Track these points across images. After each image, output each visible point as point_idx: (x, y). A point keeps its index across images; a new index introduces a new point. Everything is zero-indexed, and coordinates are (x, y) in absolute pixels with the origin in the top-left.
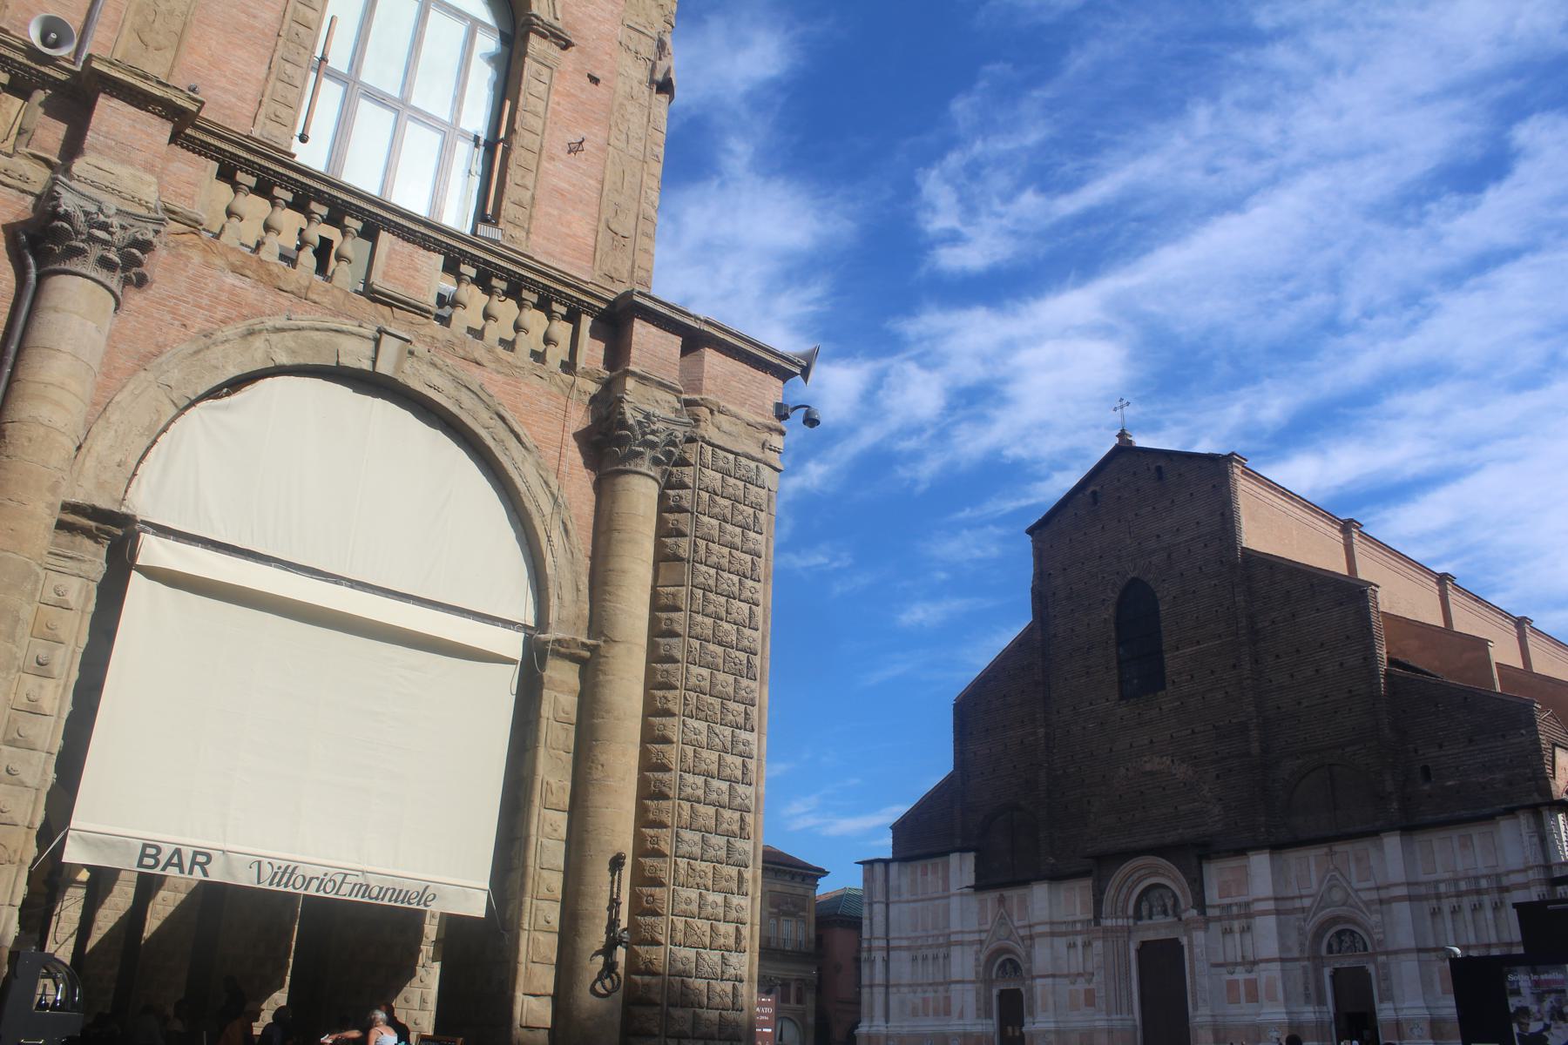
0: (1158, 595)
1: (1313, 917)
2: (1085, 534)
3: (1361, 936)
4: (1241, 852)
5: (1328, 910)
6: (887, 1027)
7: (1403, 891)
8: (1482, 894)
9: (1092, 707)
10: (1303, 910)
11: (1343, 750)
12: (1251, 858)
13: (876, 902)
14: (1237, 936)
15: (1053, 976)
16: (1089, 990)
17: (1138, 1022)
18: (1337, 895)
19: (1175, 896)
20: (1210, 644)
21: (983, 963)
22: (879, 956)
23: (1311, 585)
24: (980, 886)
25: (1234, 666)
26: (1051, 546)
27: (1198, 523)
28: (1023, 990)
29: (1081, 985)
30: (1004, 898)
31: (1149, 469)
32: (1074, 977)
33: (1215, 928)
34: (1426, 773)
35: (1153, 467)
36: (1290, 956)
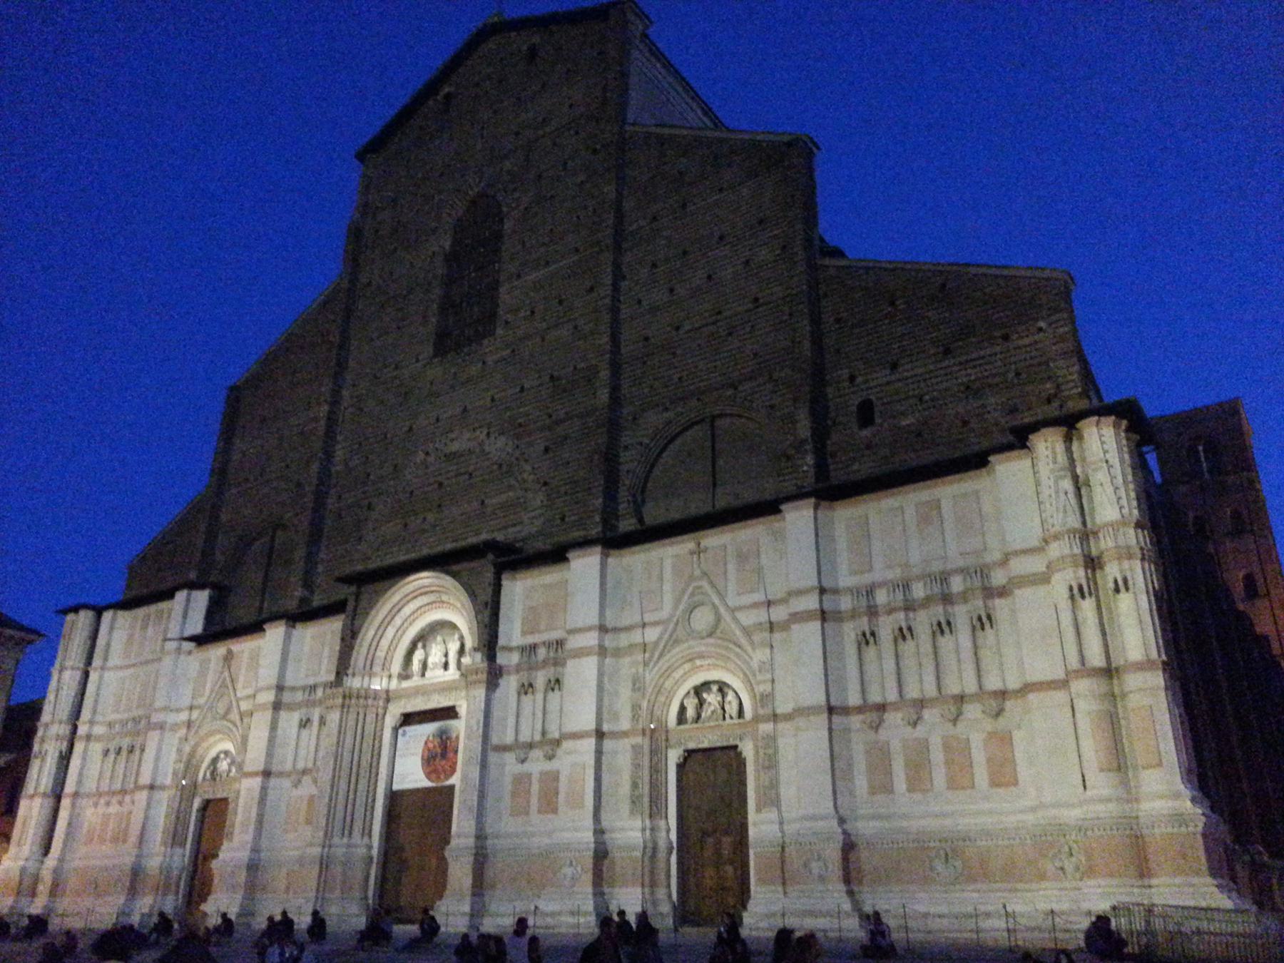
1: (659, 659)
3: (736, 693)
4: (557, 556)
8: (952, 603)
11: (736, 389)
14: (540, 696)
17: (375, 852)
19: (462, 638)
24: (201, 640)
34: (866, 414)
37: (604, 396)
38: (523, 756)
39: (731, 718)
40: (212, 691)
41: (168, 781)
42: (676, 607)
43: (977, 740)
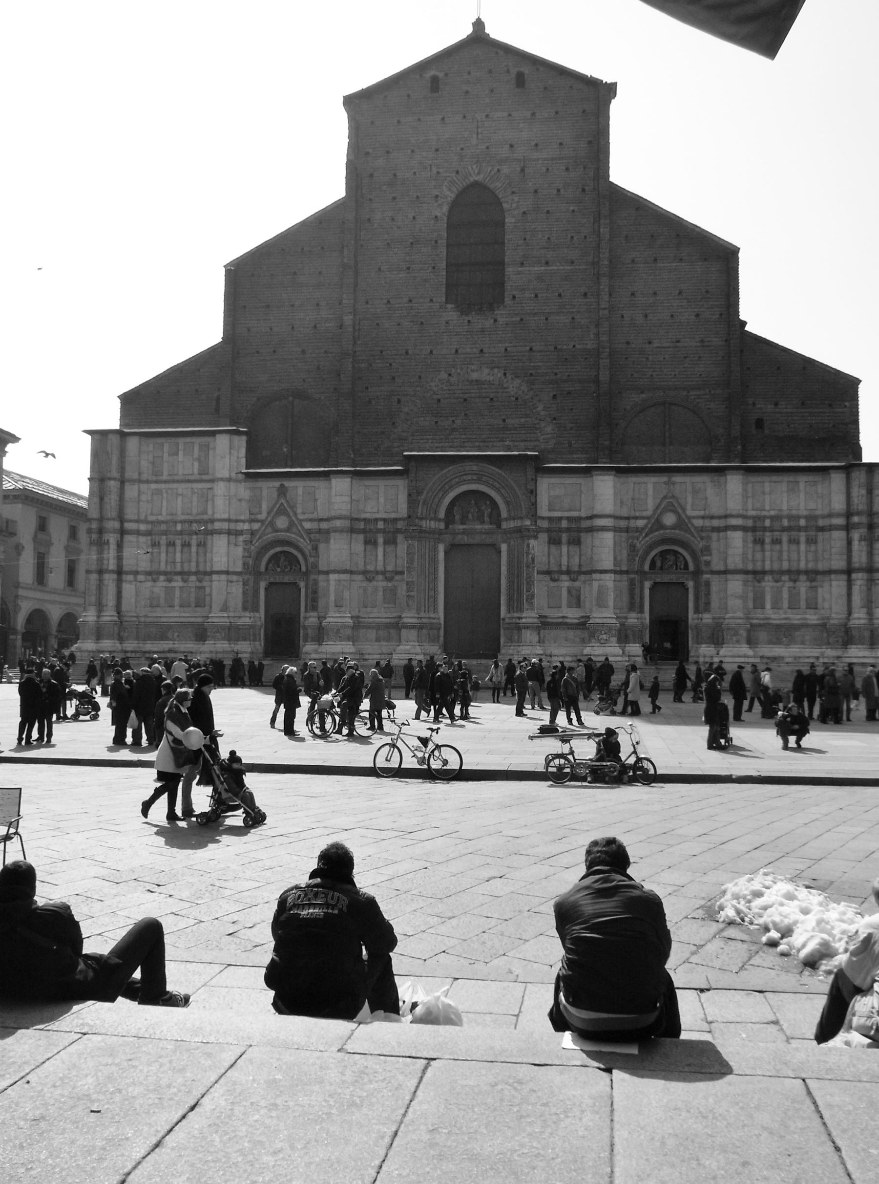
0: (505, 206)
2: (419, 120)
9: (410, 305)
10: (638, 530)
11: (688, 392)
12: (594, 477)
13: (110, 479)
14: (564, 549)
15: (352, 572)
17: (442, 622)
18: (669, 519)
20: (561, 268)
22: (112, 539)
25: (585, 295)
26: (372, 123)
27: (561, 144)
31: (508, 71)
32: (368, 575)
35: (514, 72)
36: (618, 569)
37: (604, 376)
38: (556, 577)
39: (681, 569)
40: (269, 513)
41: (239, 569)
42: (655, 511)
43: (803, 590)
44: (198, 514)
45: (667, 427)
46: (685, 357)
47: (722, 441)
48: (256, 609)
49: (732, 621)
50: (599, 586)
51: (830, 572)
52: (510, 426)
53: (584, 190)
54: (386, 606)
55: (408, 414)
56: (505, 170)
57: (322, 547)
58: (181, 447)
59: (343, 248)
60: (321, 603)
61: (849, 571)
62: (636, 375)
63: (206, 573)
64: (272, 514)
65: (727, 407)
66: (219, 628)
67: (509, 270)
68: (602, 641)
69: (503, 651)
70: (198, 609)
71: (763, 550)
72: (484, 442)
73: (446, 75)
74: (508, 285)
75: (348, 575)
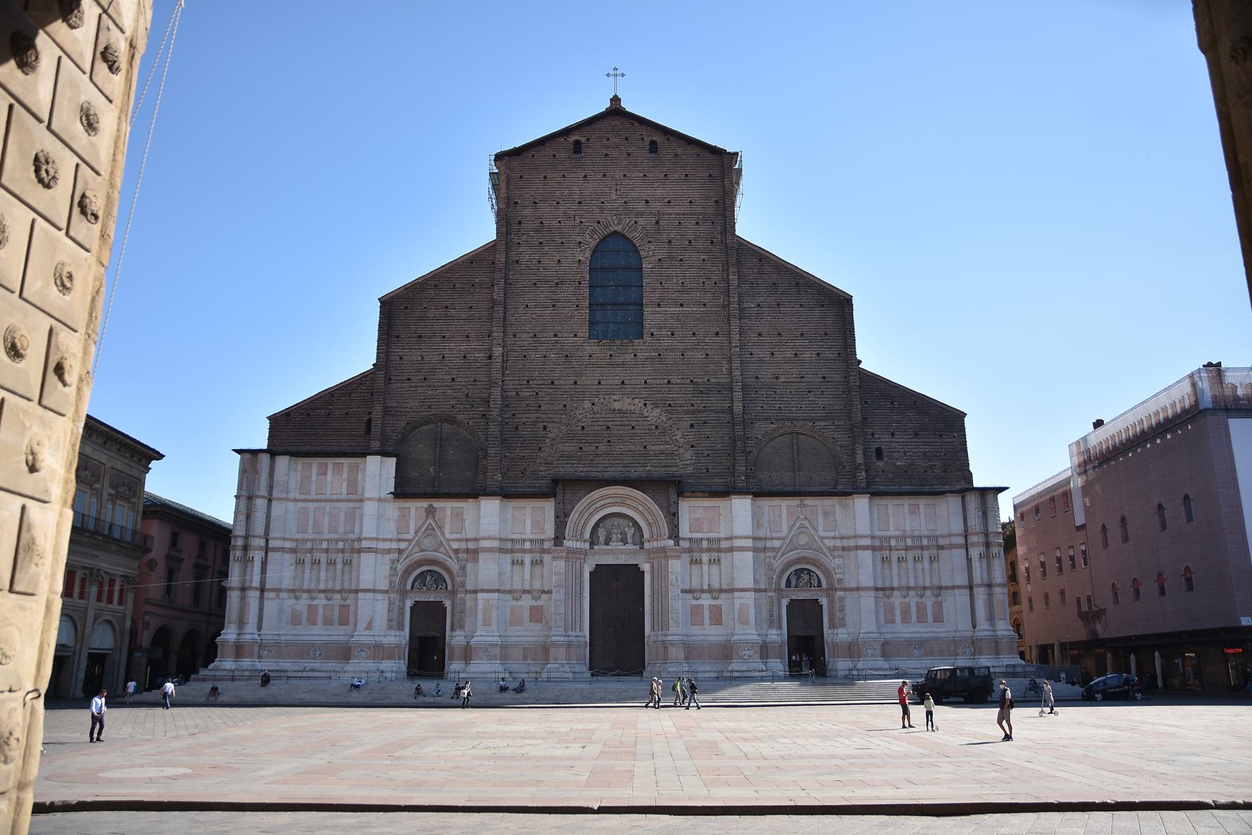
0: (642, 253)
1: (781, 557)
2: (564, 176)
3: (818, 577)
5: (796, 552)
6: (259, 635)
7: (867, 542)
10: (773, 549)
11: (814, 423)
13: (258, 497)
14: (705, 567)
15: (498, 591)
16: (535, 606)
18: (803, 540)
21: (399, 574)
22: (258, 556)
23: (797, 284)
26: (521, 177)
27: (691, 202)
28: (447, 603)
29: (527, 602)
30: (434, 508)
31: (643, 139)
33: (686, 557)
34: (879, 453)
35: (647, 140)
36: (757, 587)
37: (738, 407)
39: (814, 586)
40: (416, 533)
41: (384, 585)
44: (346, 533)
45: (796, 454)
46: (809, 392)
47: (847, 467)
48: (401, 627)
49: (865, 635)
50: (740, 604)
51: (953, 587)
52: (651, 453)
53: (712, 242)
54: (532, 624)
55: (553, 439)
56: (641, 221)
57: (469, 566)
58: (330, 467)
59: (492, 285)
60: (468, 621)
61: (971, 588)
62: (766, 407)
63: (351, 591)
64: (420, 534)
65: (849, 437)
66: (363, 646)
67: (647, 310)
68: (746, 657)
69: (648, 668)
70: (343, 627)
71: (890, 567)
72: (627, 467)
73: (588, 140)
74: (646, 324)
75: (497, 594)
